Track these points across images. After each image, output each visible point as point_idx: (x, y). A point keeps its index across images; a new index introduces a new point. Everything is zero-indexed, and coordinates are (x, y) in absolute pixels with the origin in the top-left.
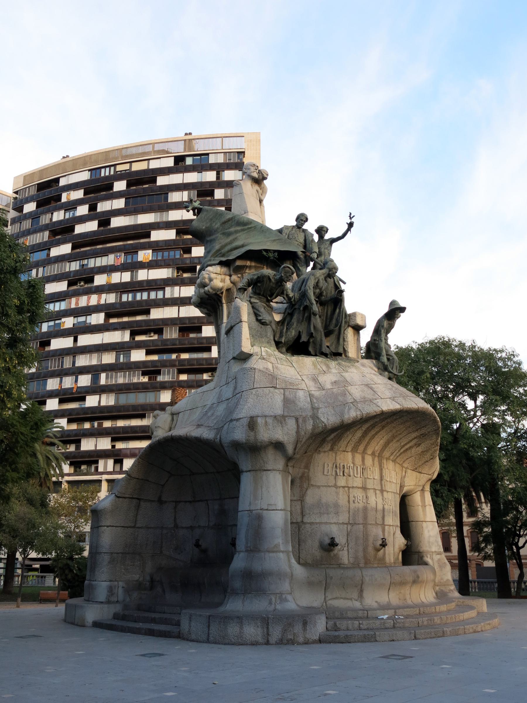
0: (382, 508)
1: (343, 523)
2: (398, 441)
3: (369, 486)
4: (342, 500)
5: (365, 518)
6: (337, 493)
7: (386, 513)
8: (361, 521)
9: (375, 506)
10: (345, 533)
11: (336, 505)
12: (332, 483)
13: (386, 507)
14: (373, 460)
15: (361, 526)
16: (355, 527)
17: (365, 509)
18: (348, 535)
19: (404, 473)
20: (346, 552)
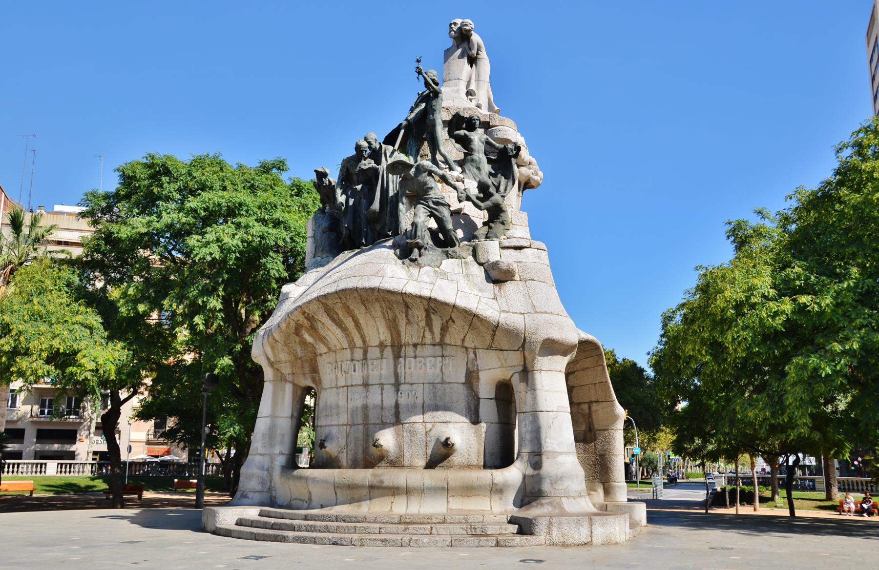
0: (393, 402)
1: (343, 425)
2: (409, 322)
3: (371, 382)
4: (342, 402)
5: (366, 417)
6: (338, 394)
7: (400, 410)
8: (360, 421)
9: (380, 403)
10: (344, 435)
11: (338, 406)
12: (334, 385)
13: (403, 401)
14: (382, 352)
15: (361, 427)
16: (354, 428)
17: (365, 407)
18: (347, 436)
19: (472, 355)
20: (345, 454)
